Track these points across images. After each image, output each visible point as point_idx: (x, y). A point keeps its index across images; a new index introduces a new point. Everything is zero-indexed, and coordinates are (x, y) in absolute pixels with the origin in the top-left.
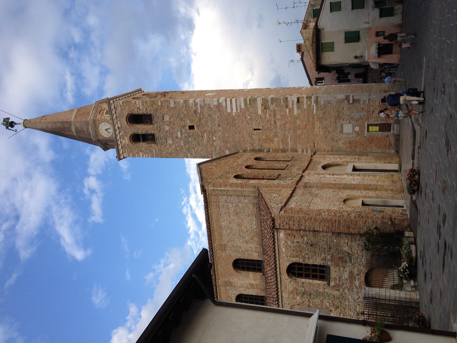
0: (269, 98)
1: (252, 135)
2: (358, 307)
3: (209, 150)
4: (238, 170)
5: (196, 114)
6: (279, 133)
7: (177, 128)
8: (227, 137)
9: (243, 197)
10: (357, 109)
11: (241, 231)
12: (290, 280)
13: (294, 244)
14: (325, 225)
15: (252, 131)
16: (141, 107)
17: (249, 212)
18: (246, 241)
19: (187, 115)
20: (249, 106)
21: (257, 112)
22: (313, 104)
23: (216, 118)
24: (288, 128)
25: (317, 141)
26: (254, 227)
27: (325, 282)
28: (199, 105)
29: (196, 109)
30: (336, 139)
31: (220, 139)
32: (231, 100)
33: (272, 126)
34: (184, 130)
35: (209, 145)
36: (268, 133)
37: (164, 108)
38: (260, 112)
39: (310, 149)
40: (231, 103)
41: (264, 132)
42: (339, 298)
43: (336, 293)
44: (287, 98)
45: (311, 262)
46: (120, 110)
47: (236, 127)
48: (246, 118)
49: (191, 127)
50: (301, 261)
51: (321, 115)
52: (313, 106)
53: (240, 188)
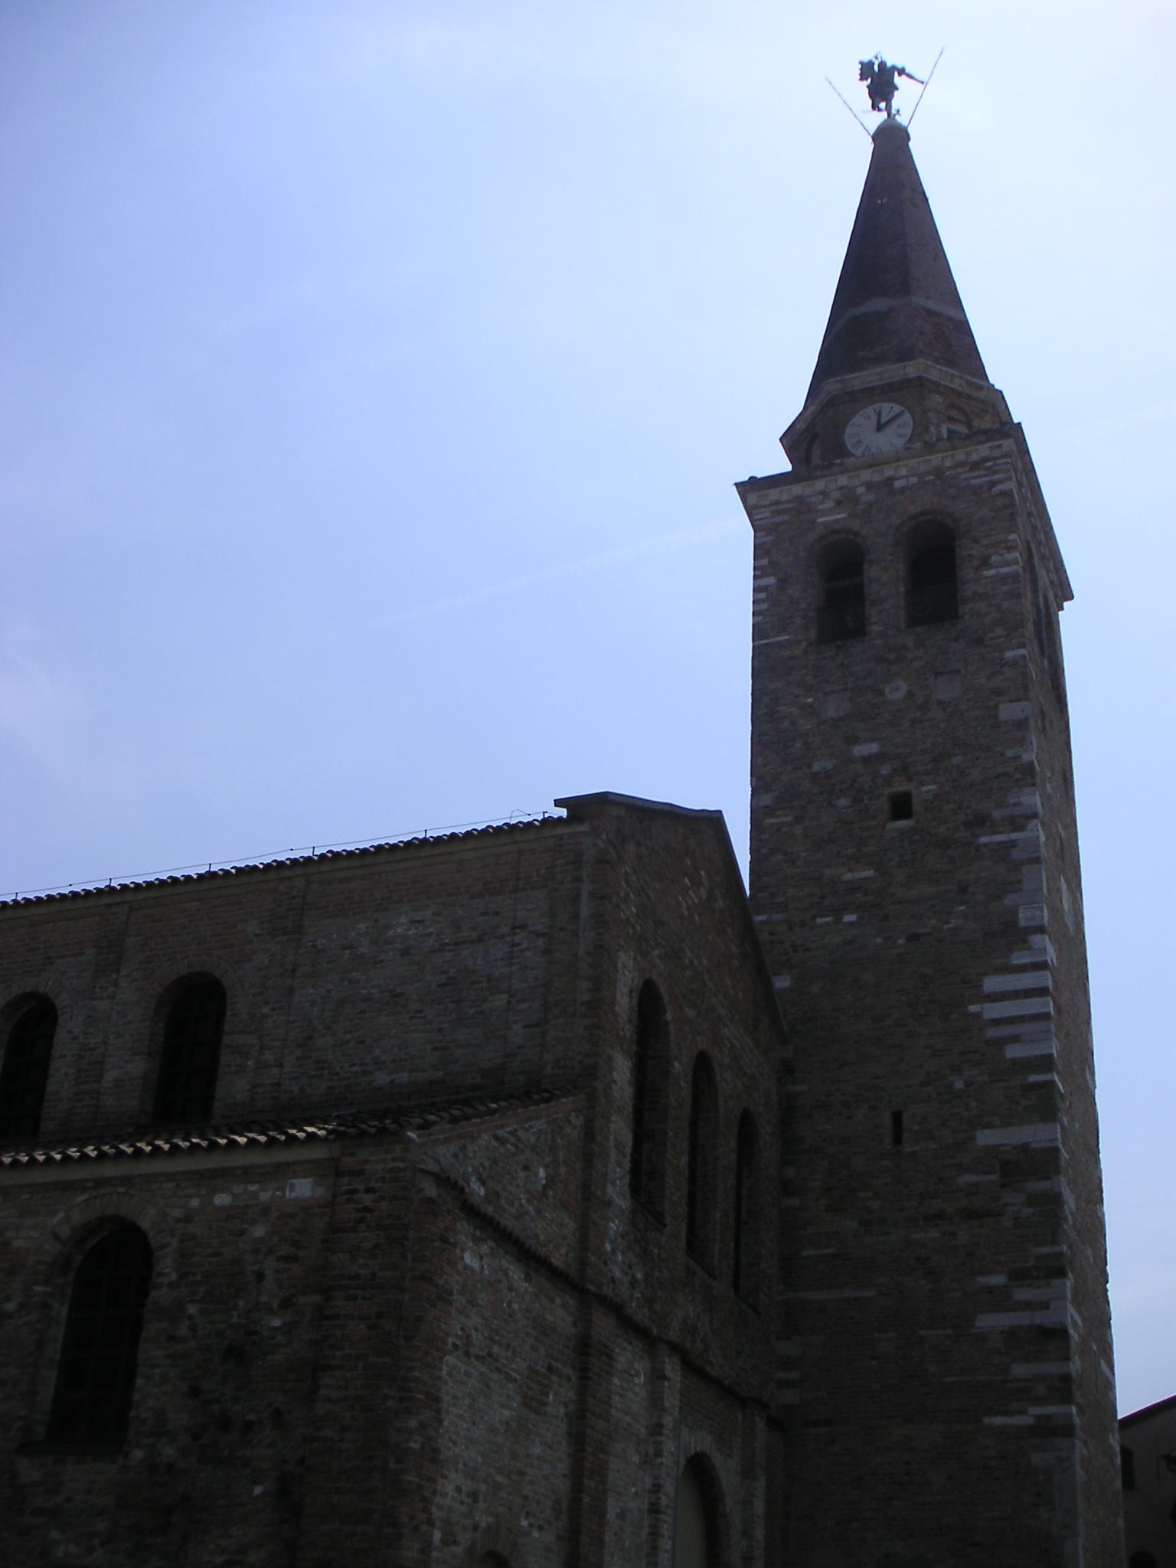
4: (690, 1013)
11: (363, 1012)
12: (65, 1232)
16: (992, 572)
18: (310, 1038)
21: (989, 1126)
22: (1035, 1410)
23: (953, 923)
26: (382, 1078)
28: (1014, 836)
32: (1043, 991)
34: (886, 770)
38: (986, 1138)
41: (886, 1163)
46: (972, 482)
49: (901, 807)
50: (161, 1296)
52: (1023, 1412)
53: (586, 997)
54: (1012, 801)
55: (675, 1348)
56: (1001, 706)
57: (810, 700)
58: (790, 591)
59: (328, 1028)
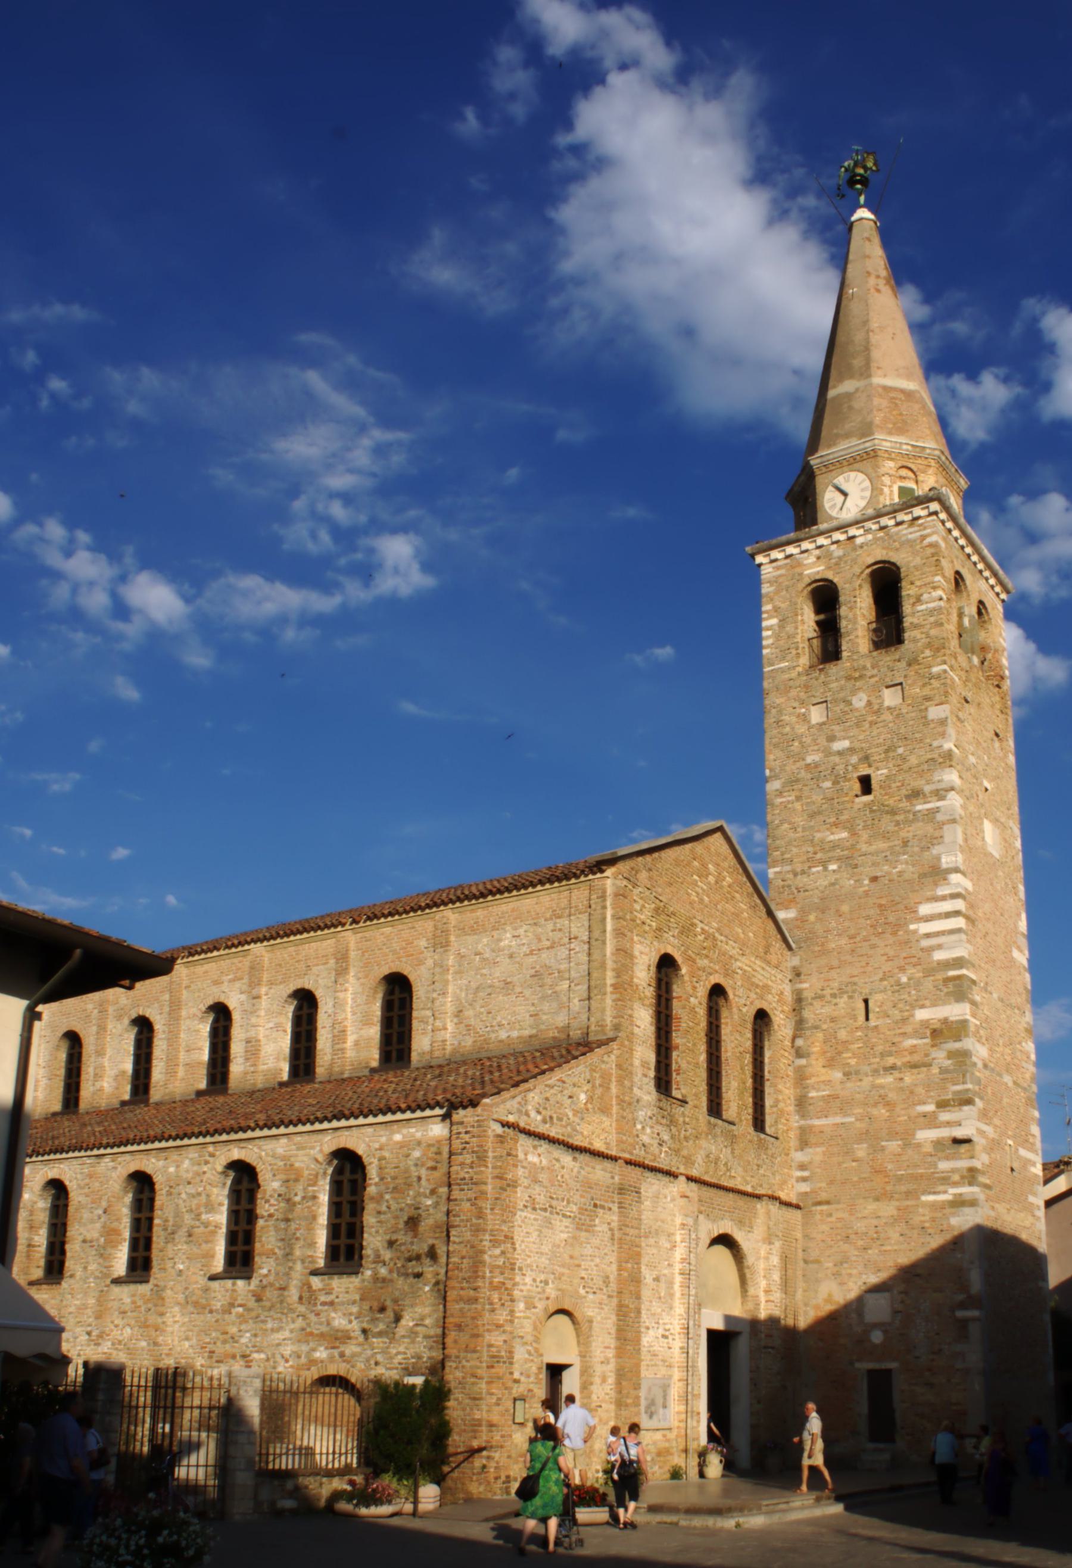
0: (968, 1043)
1: (847, 992)
3: (795, 850)
5: (908, 797)
6: (859, 1084)
7: (861, 737)
8: (837, 911)
10: (938, 1334)
11: (489, 994)
13: (413, 1168)
14: (463, 1258)
15: (861, 993)
16: (923, 607)
17: (545, 1014)
18: (461, 1011)
19: (905, 767)
20: (940, 976)
21: (923, 1007)
22: (953, 1191)
23: (900, 868)
24: (875, 1112)
25: (837, 1210)
26: (503, 1035)
29: (925, 796)
30: (844, 1272)
31: (833, 884)
32: (957, 913)
33: (877, 1060)
34: (854, 759)
35: (811, 849)
36: (857, 1046)
37: (924, 685)
39: (808, 1190)
40: (948, 915)
41: (859, 1034)
44: (969, 1102)
45: (369, 1219)
47: (872, 937)
48: (902, 969)
49: (866, 785)
50: (371, 1190)
51: (916, 1220)
52: (945, 1192)
54: (936, 778)
56: (930, 709)
57: (803, 710)
58: (788, 629)
59: (471, 1005)
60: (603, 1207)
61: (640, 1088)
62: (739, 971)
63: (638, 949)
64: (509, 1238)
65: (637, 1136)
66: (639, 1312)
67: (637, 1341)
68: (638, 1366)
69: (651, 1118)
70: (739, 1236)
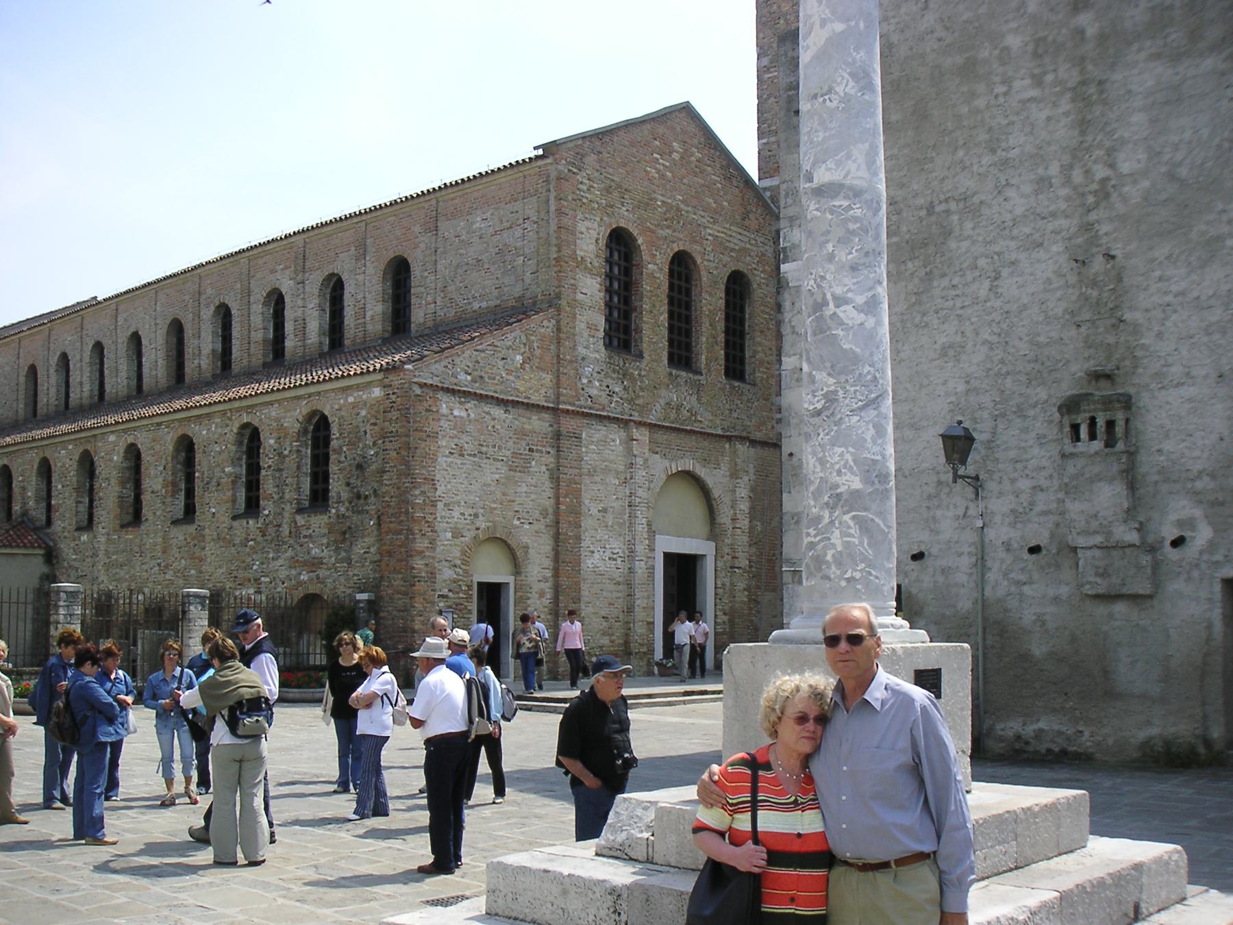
2: (268, 579)
9: (535, 269)
13: (361, 424)
14: (392, 497)
26: (476, 306)
27: (307, 503)
42: (278, 536)
43: (285, 530)
45: (333, 468)
50: (334, 444)
53: (555, 256)
55: (640, 424)
60: (537, 451)
61: (587, 347)
62: (710, 238)
63: (581, 227)
64: (432, 482)
65: (583, 389)
66: (578, 538)
67: (579, 564)
68: (578, 584)
69: (599, 373)
70: (702, 472)
